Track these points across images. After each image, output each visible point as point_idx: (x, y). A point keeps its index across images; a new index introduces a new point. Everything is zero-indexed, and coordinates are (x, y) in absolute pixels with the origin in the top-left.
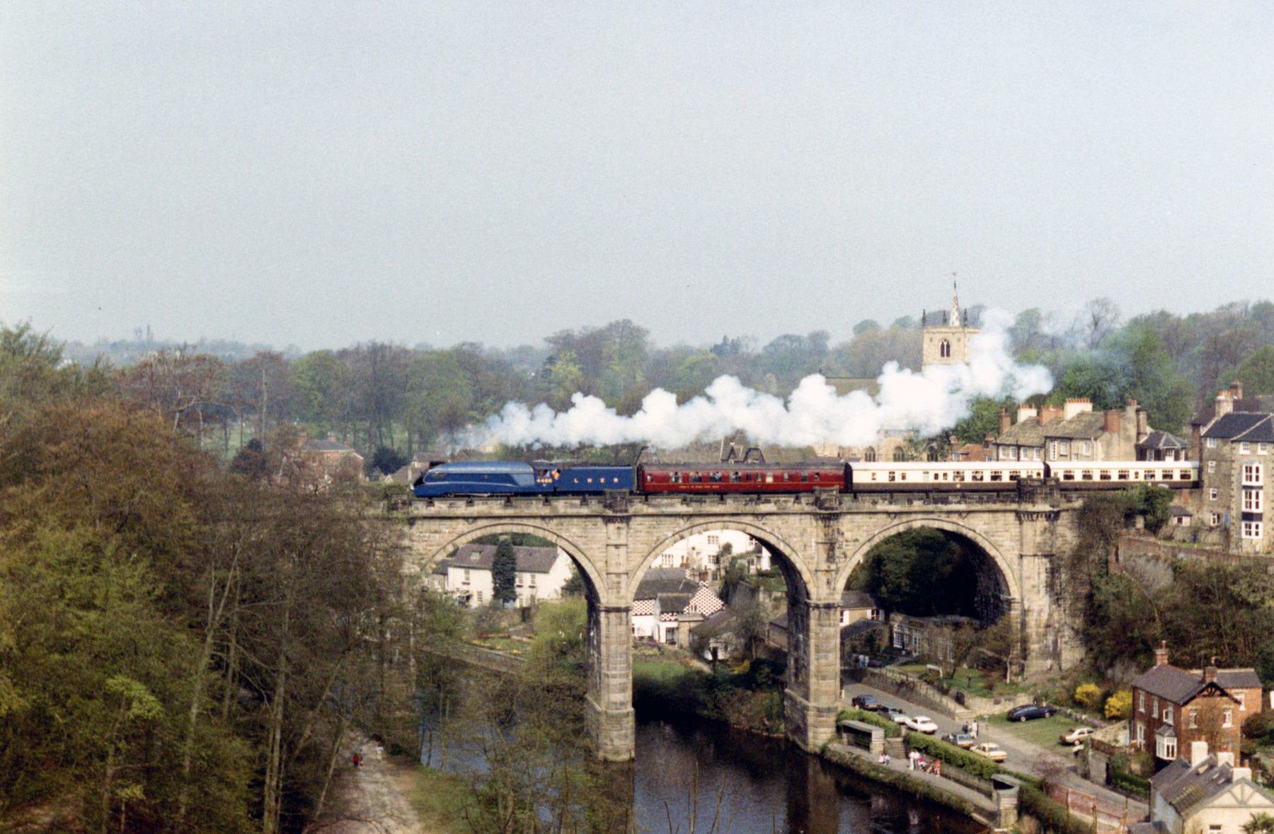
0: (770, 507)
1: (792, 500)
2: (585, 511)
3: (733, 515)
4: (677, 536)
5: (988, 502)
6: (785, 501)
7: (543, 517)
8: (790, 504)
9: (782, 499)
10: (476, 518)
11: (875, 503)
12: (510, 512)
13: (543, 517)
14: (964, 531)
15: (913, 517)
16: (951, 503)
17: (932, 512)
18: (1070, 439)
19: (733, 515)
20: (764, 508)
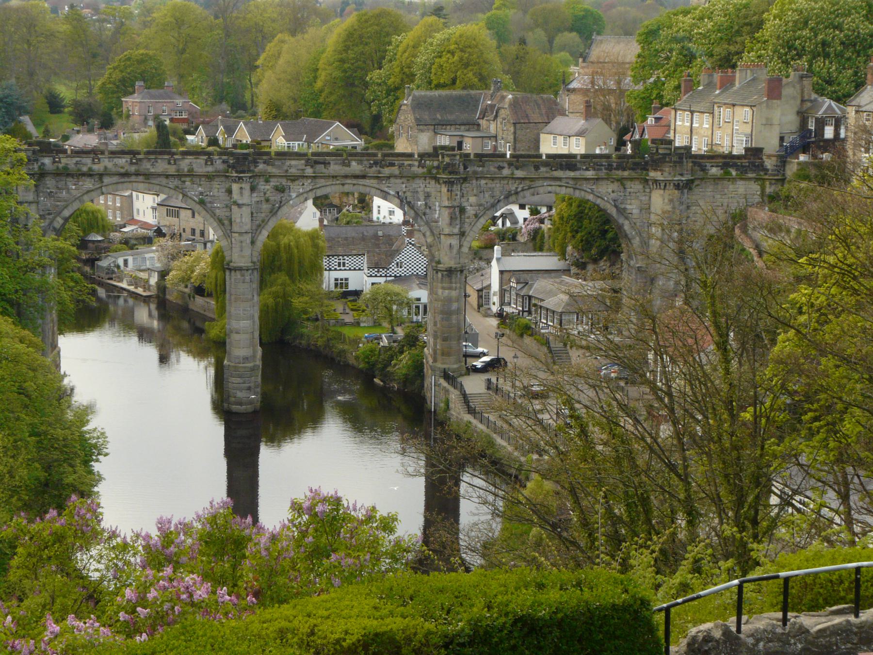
0: (395, 170)
1: (416, 163)
2: (210, 169)
3: (356, 177)
4: (302, 198)
5: (617, 169)
6: (410, 165)
7: (167, 176)
8: (413, 169)
9: (406, 163)
10: (101, 176)
11: (501, 168)
12: (133, 169)
13: (167, 176)
14: (591, 197)
15: (540, 183)
16: (579, 169)
17: (559, 179)
18: (734, 105)
19: (356, 177)
20: (387, 171)
